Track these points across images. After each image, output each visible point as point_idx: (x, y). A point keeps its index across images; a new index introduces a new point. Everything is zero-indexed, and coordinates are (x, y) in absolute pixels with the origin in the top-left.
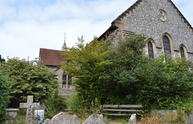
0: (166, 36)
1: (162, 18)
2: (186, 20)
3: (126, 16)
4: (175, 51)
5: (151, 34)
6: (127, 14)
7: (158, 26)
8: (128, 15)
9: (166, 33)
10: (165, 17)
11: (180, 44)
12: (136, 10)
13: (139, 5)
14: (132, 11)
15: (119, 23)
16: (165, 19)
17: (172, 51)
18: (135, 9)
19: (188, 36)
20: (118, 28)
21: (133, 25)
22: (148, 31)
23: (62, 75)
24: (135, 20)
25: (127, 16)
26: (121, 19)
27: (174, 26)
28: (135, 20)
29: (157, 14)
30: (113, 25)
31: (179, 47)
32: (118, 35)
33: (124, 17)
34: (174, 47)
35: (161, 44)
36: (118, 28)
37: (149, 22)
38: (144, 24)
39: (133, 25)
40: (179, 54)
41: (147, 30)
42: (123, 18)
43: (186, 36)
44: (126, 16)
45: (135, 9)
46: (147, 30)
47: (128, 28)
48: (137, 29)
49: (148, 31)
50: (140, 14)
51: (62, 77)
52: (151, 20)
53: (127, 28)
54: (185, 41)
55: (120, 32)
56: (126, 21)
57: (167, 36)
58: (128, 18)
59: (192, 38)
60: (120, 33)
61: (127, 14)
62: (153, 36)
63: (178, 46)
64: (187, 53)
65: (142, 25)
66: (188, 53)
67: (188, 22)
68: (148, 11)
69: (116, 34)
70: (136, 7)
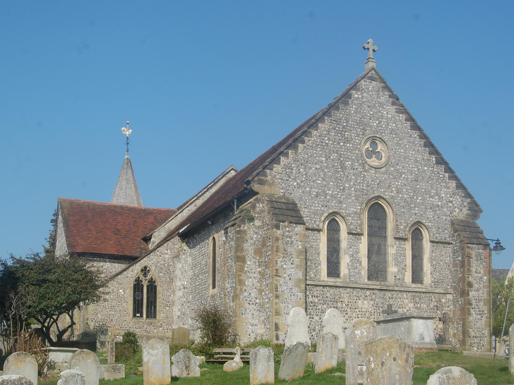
0: (377, 203)
1: (374, 158)
2: (442, 158)
3: (279, 163)
4: (396, 238)
5: (341, 202)
6: (282, 159)
7: (358, 181)
8: (285, 161)
9: (379, 197)
10: (383, 156)
11: (413, 219)
12: (305, 145)
13: (314, 132)
14: (296, 148)
15: (262, 183)
16: (383, 159)
17: (390, 240)
18: (303, 142)
19: (440, 198)
20: (258, 193)
21: (295, 184)
22: (332, 196)
23: (132, 286)
24: (302, 170)
25: (282, 164)
26: (268, 171)
27: (403, 176)
28: (302, 170)
29: (360, 150)
30: (249, 187)
31: (408, 229)
32: (258, 209)
33: (275, 165)
34: (397, 228)
35: (362, 224)
36: (258, 193)
37: (337, 172)
38: (323, 179)
39: (295, 184)
40: (408, 246)
41: (330, 192)
42: (272, 169)
43: (436, 201)
44: (279, 163)
45: (303, 142)
46: (330, 192)
47: (282, 191)
48: (303, 192)
49: (332, 196)
50: (315, 155)
51: (132, 290)
52: (343, 167)
53: (279, 192)
54: (430, 214)
55: (263, 203)
56: (278, 177)
57: (380, 204)
58: (288, 167)
59: (450, 204)
60: (261, 205)
61: (282, 159)
62: (344, 206)
63: (405, 228)
64: (429, 243)
65: (319, 182)
66: (432, 242)
67: (446, 164)
68: (339, 144)
69: (254, 207)
70: (306, 139)
